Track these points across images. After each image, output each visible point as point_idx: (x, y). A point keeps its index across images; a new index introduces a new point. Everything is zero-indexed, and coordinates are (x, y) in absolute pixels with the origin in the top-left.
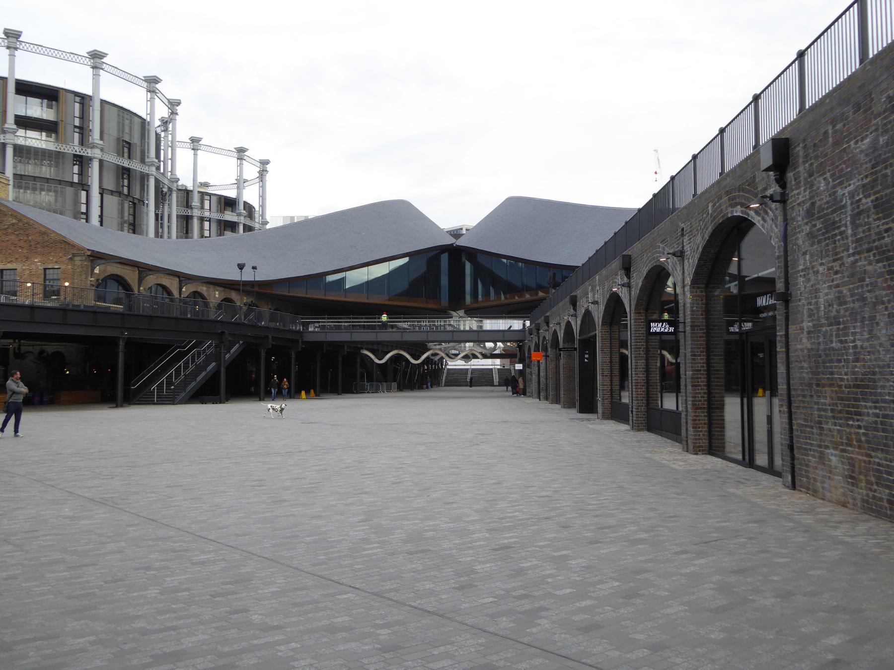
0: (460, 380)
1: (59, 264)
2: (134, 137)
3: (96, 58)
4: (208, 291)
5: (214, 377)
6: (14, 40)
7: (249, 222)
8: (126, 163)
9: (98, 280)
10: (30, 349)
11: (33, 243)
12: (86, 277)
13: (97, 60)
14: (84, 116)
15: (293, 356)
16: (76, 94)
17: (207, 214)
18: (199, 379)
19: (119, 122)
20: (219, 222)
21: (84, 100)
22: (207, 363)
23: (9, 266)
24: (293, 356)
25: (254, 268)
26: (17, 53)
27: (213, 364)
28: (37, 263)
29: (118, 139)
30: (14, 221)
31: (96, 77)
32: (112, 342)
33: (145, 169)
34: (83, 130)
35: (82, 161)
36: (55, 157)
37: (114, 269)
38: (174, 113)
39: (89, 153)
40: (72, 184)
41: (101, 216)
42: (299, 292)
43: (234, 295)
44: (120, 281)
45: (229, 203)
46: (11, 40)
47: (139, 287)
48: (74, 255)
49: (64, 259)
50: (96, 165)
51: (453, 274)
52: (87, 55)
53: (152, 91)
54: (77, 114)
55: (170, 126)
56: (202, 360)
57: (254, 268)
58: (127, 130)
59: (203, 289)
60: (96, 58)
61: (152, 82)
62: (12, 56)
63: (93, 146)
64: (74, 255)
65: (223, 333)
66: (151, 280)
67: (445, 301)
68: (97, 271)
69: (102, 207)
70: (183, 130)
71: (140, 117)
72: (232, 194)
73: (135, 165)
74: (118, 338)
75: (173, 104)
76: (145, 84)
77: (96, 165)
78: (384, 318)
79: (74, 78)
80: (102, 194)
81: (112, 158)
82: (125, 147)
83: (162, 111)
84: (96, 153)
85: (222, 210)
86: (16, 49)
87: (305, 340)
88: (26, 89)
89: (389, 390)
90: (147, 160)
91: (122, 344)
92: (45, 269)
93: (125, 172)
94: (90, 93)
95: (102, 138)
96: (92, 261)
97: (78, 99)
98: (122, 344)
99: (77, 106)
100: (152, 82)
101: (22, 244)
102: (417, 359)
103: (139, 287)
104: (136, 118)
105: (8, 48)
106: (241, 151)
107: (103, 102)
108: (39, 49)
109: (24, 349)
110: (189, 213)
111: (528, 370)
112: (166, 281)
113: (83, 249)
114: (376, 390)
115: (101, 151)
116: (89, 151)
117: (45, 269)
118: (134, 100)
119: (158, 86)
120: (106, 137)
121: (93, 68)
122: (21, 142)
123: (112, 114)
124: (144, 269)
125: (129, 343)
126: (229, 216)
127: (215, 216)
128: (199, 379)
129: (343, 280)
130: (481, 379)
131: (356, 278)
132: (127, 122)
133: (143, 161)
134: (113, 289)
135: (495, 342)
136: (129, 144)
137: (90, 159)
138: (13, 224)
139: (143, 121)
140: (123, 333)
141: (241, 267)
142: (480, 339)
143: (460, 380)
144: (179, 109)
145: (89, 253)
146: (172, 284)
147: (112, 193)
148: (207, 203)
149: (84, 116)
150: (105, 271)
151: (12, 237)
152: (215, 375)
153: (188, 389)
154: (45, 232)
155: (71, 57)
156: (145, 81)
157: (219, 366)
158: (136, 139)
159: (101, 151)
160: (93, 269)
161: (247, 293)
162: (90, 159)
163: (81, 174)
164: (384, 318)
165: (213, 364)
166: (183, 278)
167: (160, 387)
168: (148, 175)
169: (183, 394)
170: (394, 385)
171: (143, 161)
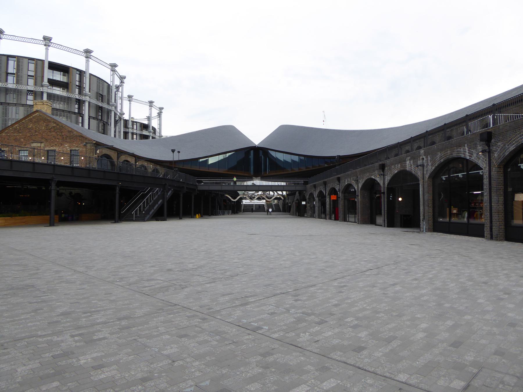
0: (250, 209)
1: (79, 148)
2: (105, 92)
3: (88, 53)
4: (147, 164)
5: (161, 208)
6: (48, 42)
7: (154, 136)
8: (100, 104)
9: (98, 156)
10: (64, 191)
11: (64, 136)
12: (93, 155)
13: (88, 54)
14: (81, 81)
15: (181, 196)
16: (78, 70)
17: (135, 131)
18: (155, 208)
21: (81, 73)
22: (157, 200)
23: (52, 148)
24: (181, 196)
25: (179, 152)
26: (49, 48)
27: (161, 201)
28: (67, 147)
29: (97, 93)
30: (55, 125)
31: (87, 62)
32: (112, 188)
33: (110, 108)
34: (81, 88)
35: (80, 103)
36: (67, 100)
37: (106, 151)
38: (122, 82)
39: (84, 98)
40: (75, 113)
42: (188, 167)
43: (158, 167)
44: (108, 157)
45: (145, 127)
46: (46, 41)
48: (87, 143)
49: (81, 145)
50: (87, 104)
51: (254, 160)
53: (113, 71)
54: (77, 79)
55: (121, 88)
56: (155, 197)
57: (179, 152)
58: (101, 89)
59: (145, 164)
60: (88, 53)
61: (113, 66)
62: (47, 49)
64: (87, 143)
65: (165, 184)
66: (123, 158)
67: (252, 173)
68: (98, 152)
70: (127, 90)
71: (107, 83)
72: (146, 122)
73: (105, 105)
74: (116, 186)
76: (110, 67)
77: (87, 104)
78: (235, 179)
79: (76, 62)
80: (89, 119)
81: (94, 101)
82: (100, 97)
83: (117, 82)
84: (87, 99)
85: (141, 130)
86: (49, 46)
87: (199, 189)
88: (53, 66)
89: (228, 214)
91: (118, 189)
92: (71, 150)
94: (84, 70)
96: (96, 147)
97: (78, 72)
98: (118, 189)
99: (78, 76)
100: (113, 66)
101: (59, 137)
102: (234, 199)
105: (45, 45)
106: (151, 103)
107: (90, 75)
108: (60, 47)
109: (61, 191)
112: (130, 159)
113: (92, 140)
114: (223, 214)
116: (84, 97)
117: (71, 150)
118: (105, 75)
119: (116, 68)
120: (91, 91)
121: (86, 57)
122: (50, 91)
123: (94, 80)
124: (120, 152)
125: (121, 190)
126: (145, 133)
127: (139, 132)
128: (155, 208)
129: (207, 161)
130: (260, 209)
131: (211, 160)
132: (101, 85)
133: (108, 104)
134: (105, 161)
135: (282, 191)
137: (84, 102)
138: (54, 127)
139: (109, 85)
140: (118, 183)
141: (173, 151)
142: (257, 190)
143: (250, 209)
144: (125, 80)
145: (94, 142)
146: (132, 160)
147: (94, 118)
148: (135, 126)
149: (81, 81)
150: (102, 152)
151: (54, 133)
152: (162, 206)
153: (151, 213)
154: (71, 131)
155: (75, 51)
157: (163, 201)
158: (105, 93)
160: (96, 151)
161: (164, 166)
162: (84, 102)
163: (79, 108)
164: (235, 179)
165: (161, 201)
166: (138, 158)
167: (136, 212)
168: (111, 111)
169: (148, 216)
170: (231, 211)
171: (108, 104)
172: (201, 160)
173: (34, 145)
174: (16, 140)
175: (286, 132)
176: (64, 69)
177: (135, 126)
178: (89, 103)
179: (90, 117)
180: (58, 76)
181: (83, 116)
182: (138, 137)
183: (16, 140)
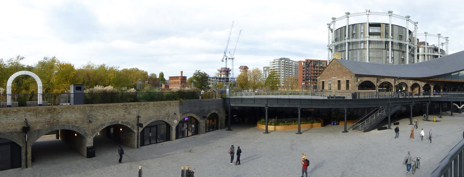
17: (430, 54)
21: (387, 25)
34: (387, 33)
35: (387, 43)
36: (380, 42)
39: (388, 40)
40: (383, 49)
45: (436, 50)
50: (390, 43)
75: (416, 24)
76: (406, 19)
84: (390, 40)
88: (371, 25)
93: (400, 45)
107: (392, 25)
126: (436, 54)
137: (389, 42)
148: (430, 51)
160: (357, 81)
161: (424, 81)
162: (389, 42)
168: (406, 45)
172: (452, 74)
173: (333, 78)
174: (327, 75)
176: (378, 25)
177: (430, 51)
178: (392, 42)
180: (376, 30)
182: (432, 57)
183: (327, 75)
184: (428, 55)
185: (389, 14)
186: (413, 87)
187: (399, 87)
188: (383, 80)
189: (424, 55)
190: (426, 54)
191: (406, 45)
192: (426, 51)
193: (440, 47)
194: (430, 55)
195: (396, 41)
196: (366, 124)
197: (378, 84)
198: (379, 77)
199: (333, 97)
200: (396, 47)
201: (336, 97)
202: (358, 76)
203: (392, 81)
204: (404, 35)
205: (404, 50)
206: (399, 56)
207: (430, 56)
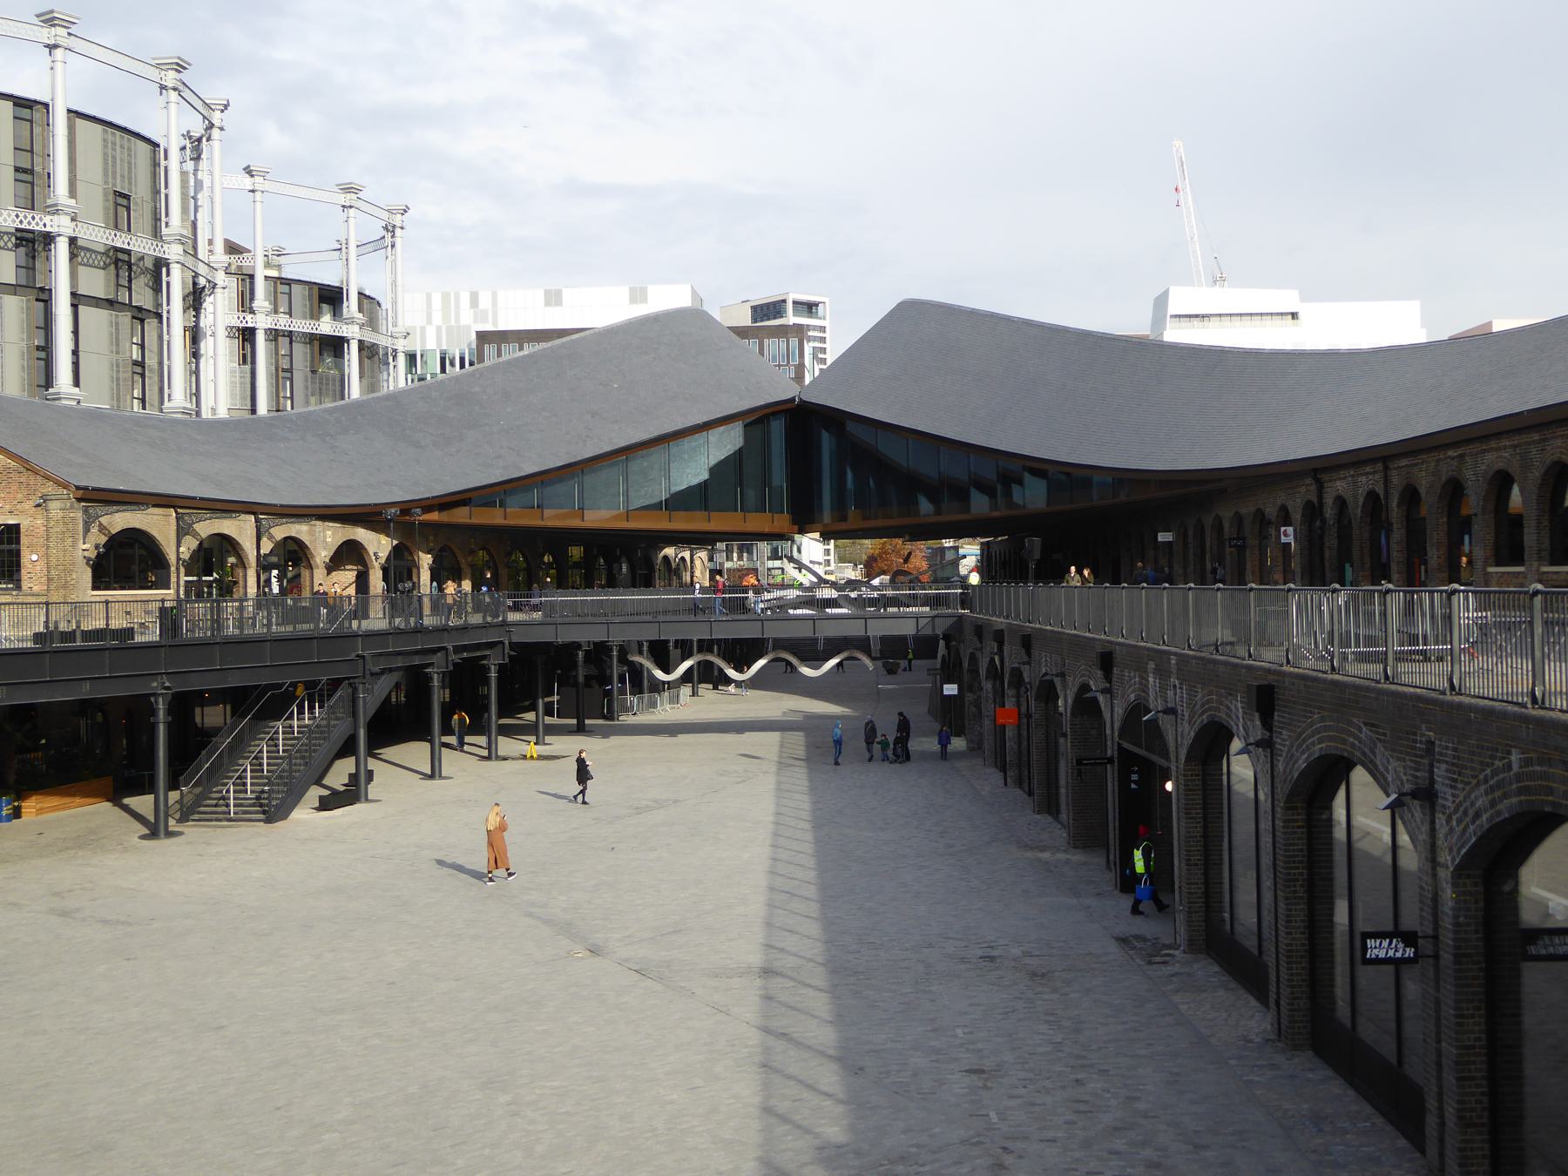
7: (369, 337)
8: (121, 241)
12: (74, 546)
17: (283, 322)
19: (105, 154)
20: (312, 338)
41: (75, 353)
43: (362, 534)
47: (178, 546)
50: (62, 249)
52: (36, 21)
63: (54, 210)
69: (76, 332)
73: (140, 244)
77: (62, 249)
80: (75, 306)
84: (59, 225)
85: (315, 315)
90: (164, 231)
93: (119, 260)
95: (72, 193)
103: (178, 546)
104: (141, 144)
107: (74, 114)
110: (250, 321)
111: (969, 697)
115: (73, 216)
116: (47, 219)
120: (80, 187)
126: (326, 325)
127: (302, 325)
133: (156, 234)
136: (127, 197)
137: (49, 239)
147: (96, 302)
156: (157, 66)
159: (73, 216)
162: (49, 239)
175: (916, 327)
178: (73, 241)
179: (77, 300)
181: (45, 297)
184: (274, 335)
185: (47, 34)
186: (349, 553)
187: (214, 556)
188: (207, 527)
189: (247, 335)
190: (262, 321)
191: (160, 264)
192: (261, 301)
193: (357, 278)
194: (290, 335)
195: (98, 235)
196: (247, 777)
197: (189, 546)
198: (183, 505)
199: (69, 636)
200: (96, 282)
201: (88, 635)
202: (96, 498)
203: (241, 529)
204: (140, 192)
205: (142, 296)
206: (116, 341)
207: (283, 341)
